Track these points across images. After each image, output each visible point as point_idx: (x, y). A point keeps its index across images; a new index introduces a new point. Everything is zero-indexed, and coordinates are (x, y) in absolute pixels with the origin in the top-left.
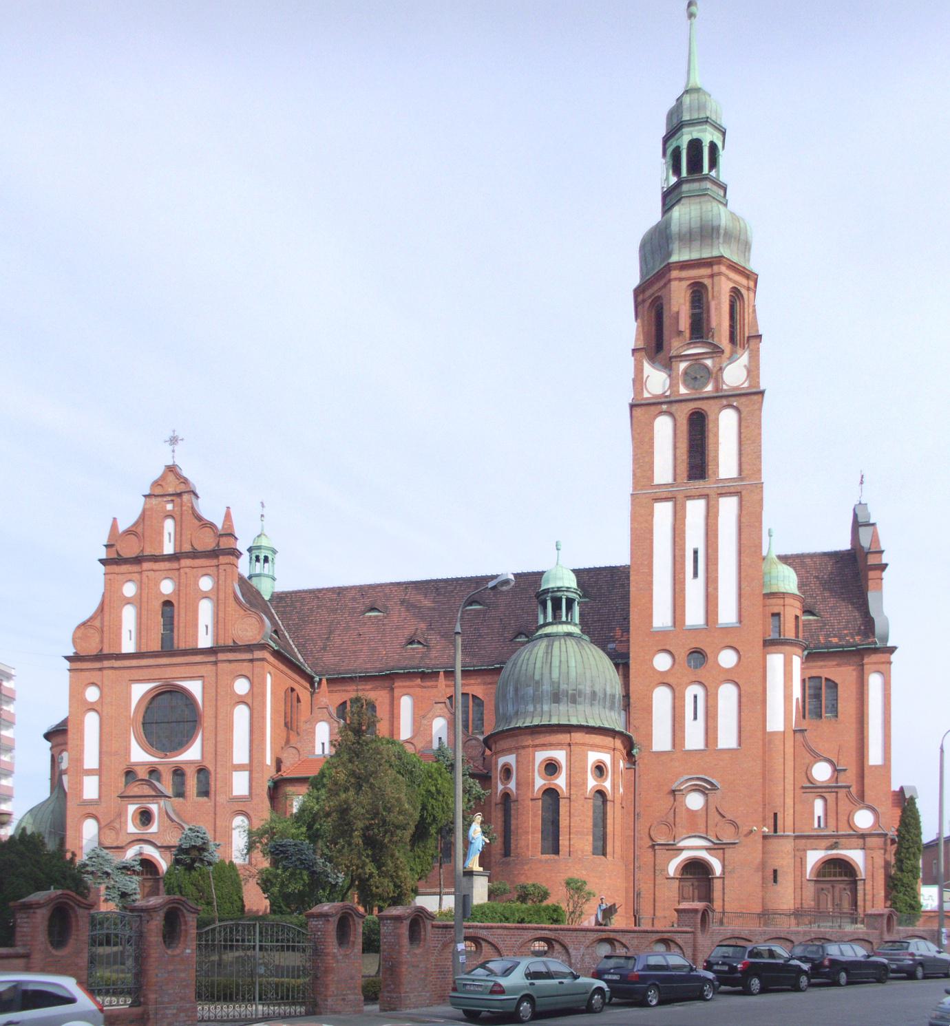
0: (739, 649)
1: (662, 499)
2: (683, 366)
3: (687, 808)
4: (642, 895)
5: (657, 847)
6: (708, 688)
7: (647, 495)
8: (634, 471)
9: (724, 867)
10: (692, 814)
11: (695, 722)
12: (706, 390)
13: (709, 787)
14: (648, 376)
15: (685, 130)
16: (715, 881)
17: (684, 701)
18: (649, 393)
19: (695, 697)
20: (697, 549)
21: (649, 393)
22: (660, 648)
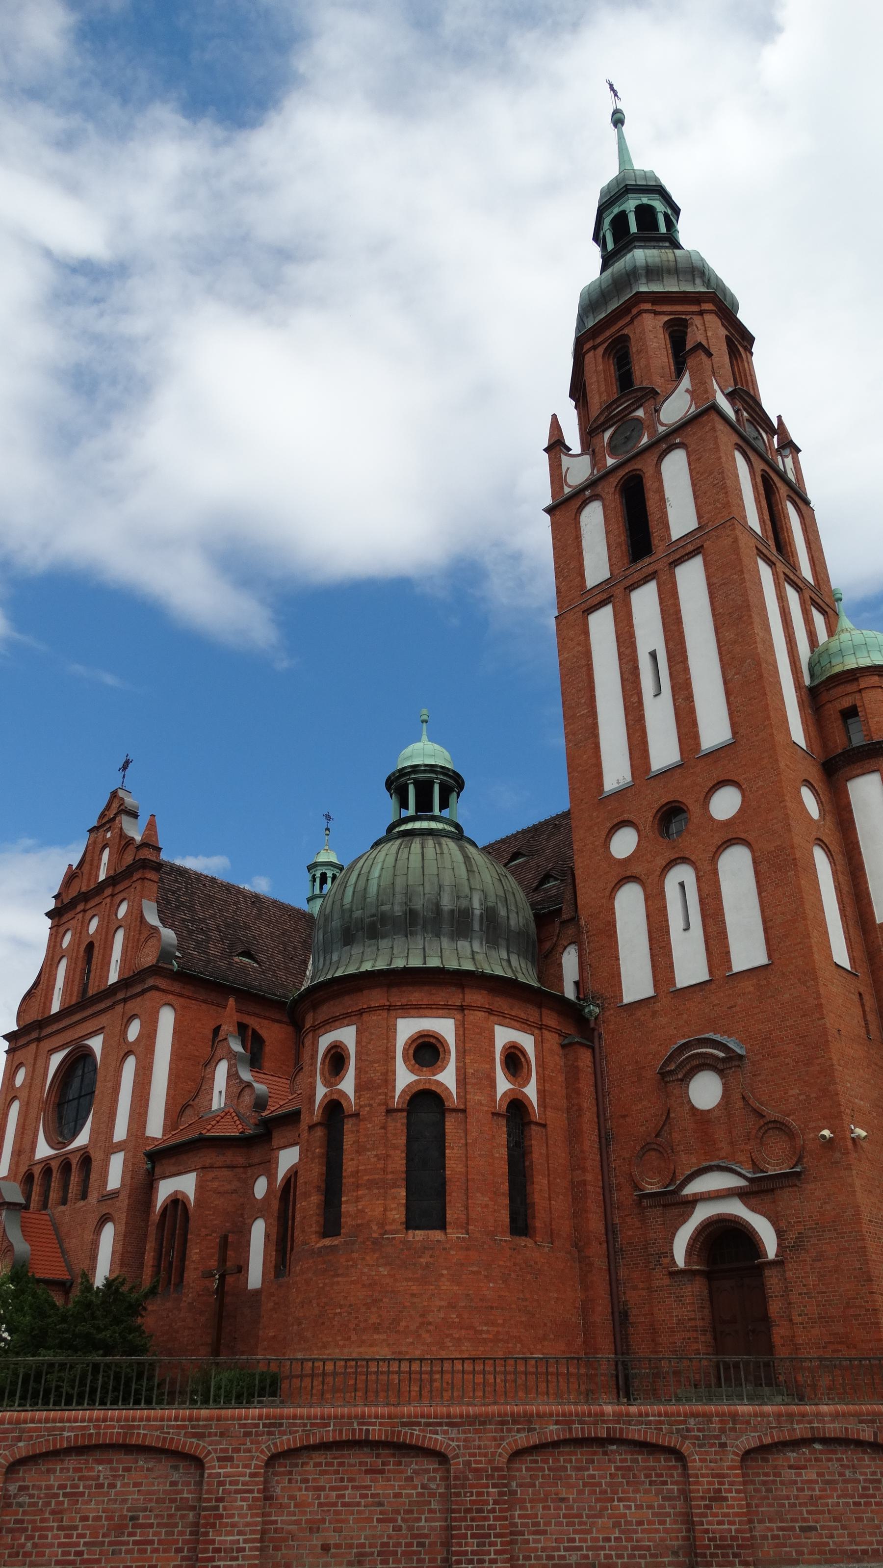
0: (740, 779)
1: (595, 605)
2: (607, 435)
3: (693, 1107)
4: (632, 1319)
5: (645, 1202)
6: (698, 864)
7: (577, 609)
8: (557, 587)
9: (780, 1234)
10: (701, 1117)
11: (687, 933)
12: (642, 443)
13: (722, 1055)
14: (568, 469)
15: (604, 215)
16: (767, 1272)
17: (664, 898)
18: (570, 486)
19: (682, 885)
20: (655, 651)
21: (570, 486)
22: (616, 821)
